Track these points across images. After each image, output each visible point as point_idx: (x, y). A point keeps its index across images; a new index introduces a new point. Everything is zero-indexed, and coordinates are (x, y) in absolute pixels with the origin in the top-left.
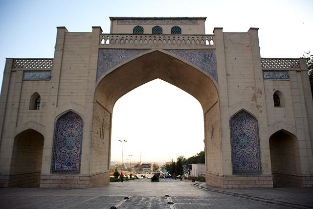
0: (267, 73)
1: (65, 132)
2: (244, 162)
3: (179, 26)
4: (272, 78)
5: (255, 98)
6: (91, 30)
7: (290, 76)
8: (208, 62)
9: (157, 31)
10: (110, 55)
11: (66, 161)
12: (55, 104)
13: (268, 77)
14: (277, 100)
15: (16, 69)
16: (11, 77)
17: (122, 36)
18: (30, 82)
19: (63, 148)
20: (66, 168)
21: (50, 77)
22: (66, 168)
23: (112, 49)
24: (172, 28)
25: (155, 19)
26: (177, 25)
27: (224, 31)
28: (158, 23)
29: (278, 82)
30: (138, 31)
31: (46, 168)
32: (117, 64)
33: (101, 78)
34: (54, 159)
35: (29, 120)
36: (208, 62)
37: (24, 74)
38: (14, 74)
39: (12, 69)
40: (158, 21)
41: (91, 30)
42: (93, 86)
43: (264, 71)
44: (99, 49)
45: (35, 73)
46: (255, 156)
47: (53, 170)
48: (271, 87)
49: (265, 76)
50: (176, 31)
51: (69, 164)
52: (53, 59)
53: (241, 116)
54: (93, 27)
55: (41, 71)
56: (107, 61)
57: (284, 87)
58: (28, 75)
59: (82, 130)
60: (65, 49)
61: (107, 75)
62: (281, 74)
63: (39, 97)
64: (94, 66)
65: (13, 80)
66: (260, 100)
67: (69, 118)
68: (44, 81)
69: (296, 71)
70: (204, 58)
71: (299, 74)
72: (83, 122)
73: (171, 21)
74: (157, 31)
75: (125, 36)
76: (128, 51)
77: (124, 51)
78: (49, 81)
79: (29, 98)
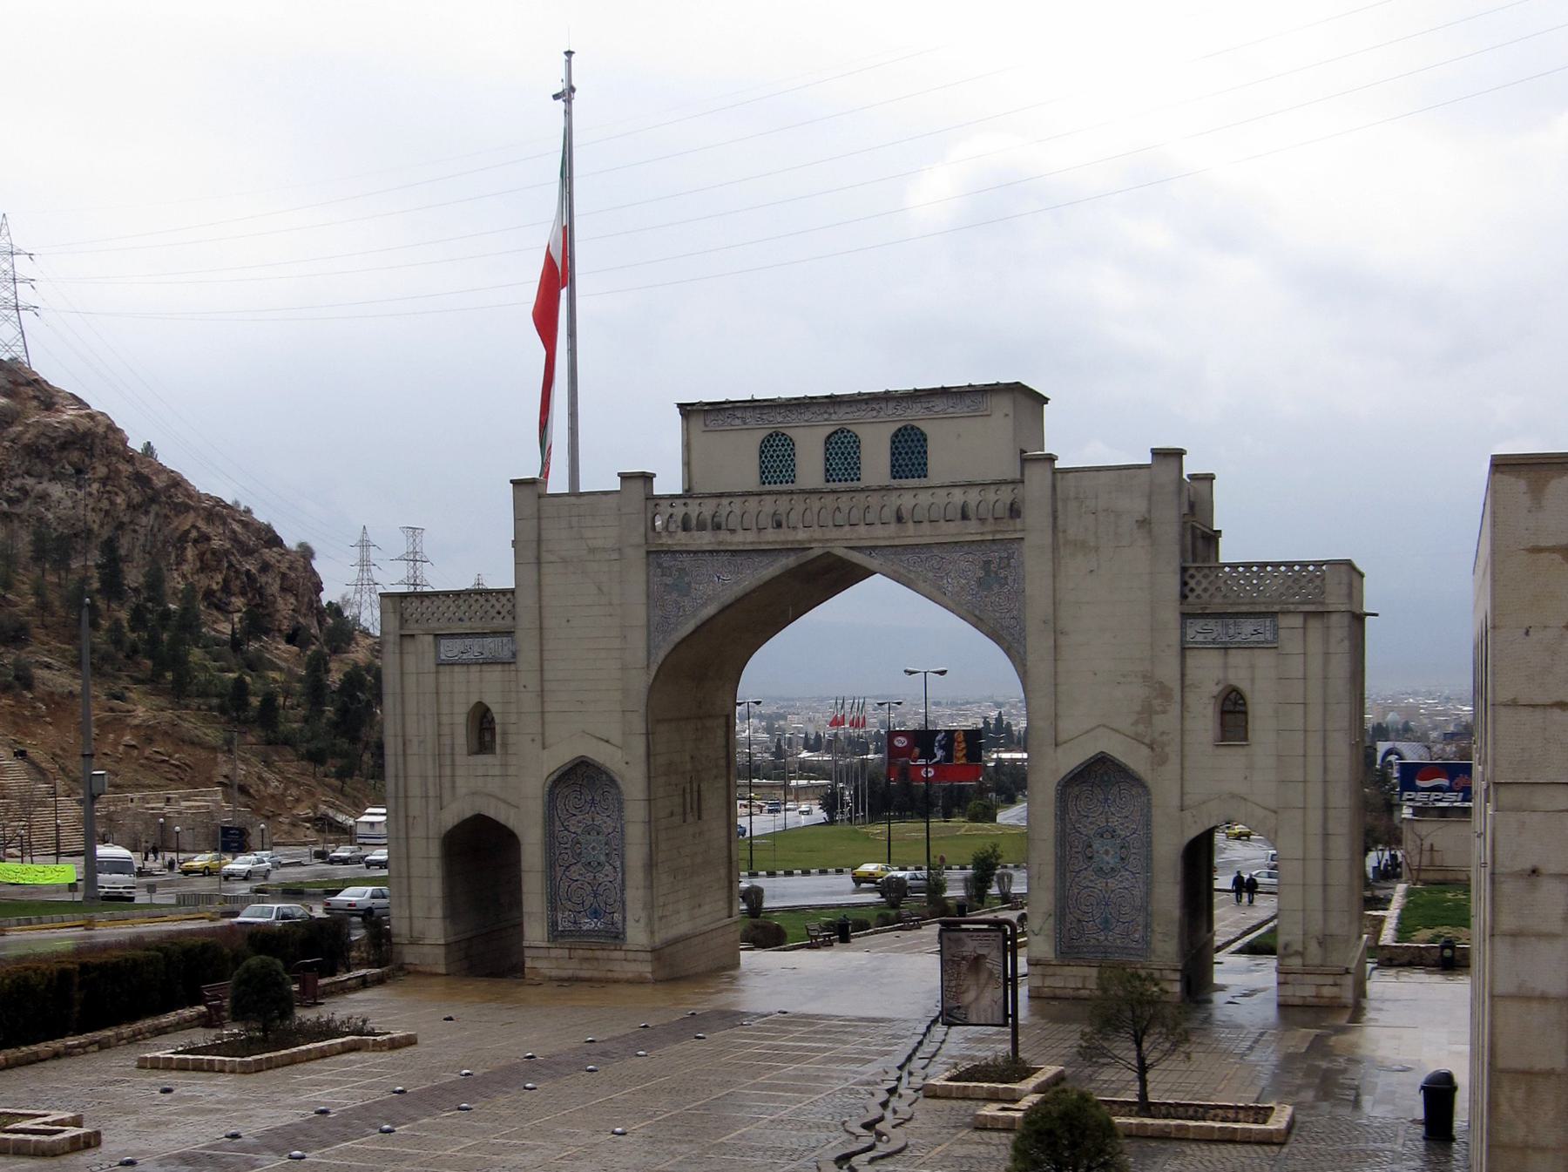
0: (1199, 624)
1: (574, 820)
2: (1106, 921)
3: (916, 424)
4: (1214, 641)
5: (1147, 713)
6: (615, 485)
7: (1281, 632)
8: (996, 588)
9: (842, 454)
10: (682, 571)
11: (587, 903)
12: (538, 738)
13: (1200, 638)
14: (1233, 712)
15: (412, 628)
16: (401, 653)
17: (715, 501)
18: (457, 668)
19: (573, 868)
20: (588, 924)
21: (514, 655)
22: (588, 924)
23: (689, 552)
24: (895, 435)
25: (833, 401)
26: (909, 423)
27: (1058, 465)
28: (842, 417)
29: (1237, 658)
30: (776, 457)
31: (534, 932)
32: (704, 605)
33: (661, 655)
34: (553, 901)
35: (476, 789)
36: (996, 588)
37: (437, 646)
38: (409, 646)
39: (401, 628)
40: (844, 409)
41: (615, 485)
42: (640, 682)
43: (1185, 616)
44: (648, 553)
45: (468, 641)
46: (1138, 902)
47: (555, 934)
48: (1209, 672)
49: (1190, 632)
50: (909, 453)
51: (596, 914)
52: (512, 592)
53: (1099, 774)
54: (624, 477)
55: (484, 635)
56: (675, 595)
57: (1257, 676)
58: (450, 649)
59: (621, 818)
60: (546, 557)
61: (684, 640)
62: (1248, 627)
63: (488, 710)
64: (639, 614)
65: (410, 662)
66: (1167, 722)
67: (580, 779)
68: (499, 667)
69: (1307, 614)
70: (981, 574)
71: (1314, 624)
72: (620, 793)
73: (892, 405)
74: (842, 454)
75: (725, 501)
76: (738, 559)
77: (725, 558)
78: (513, 667)
79: (461, 719)
